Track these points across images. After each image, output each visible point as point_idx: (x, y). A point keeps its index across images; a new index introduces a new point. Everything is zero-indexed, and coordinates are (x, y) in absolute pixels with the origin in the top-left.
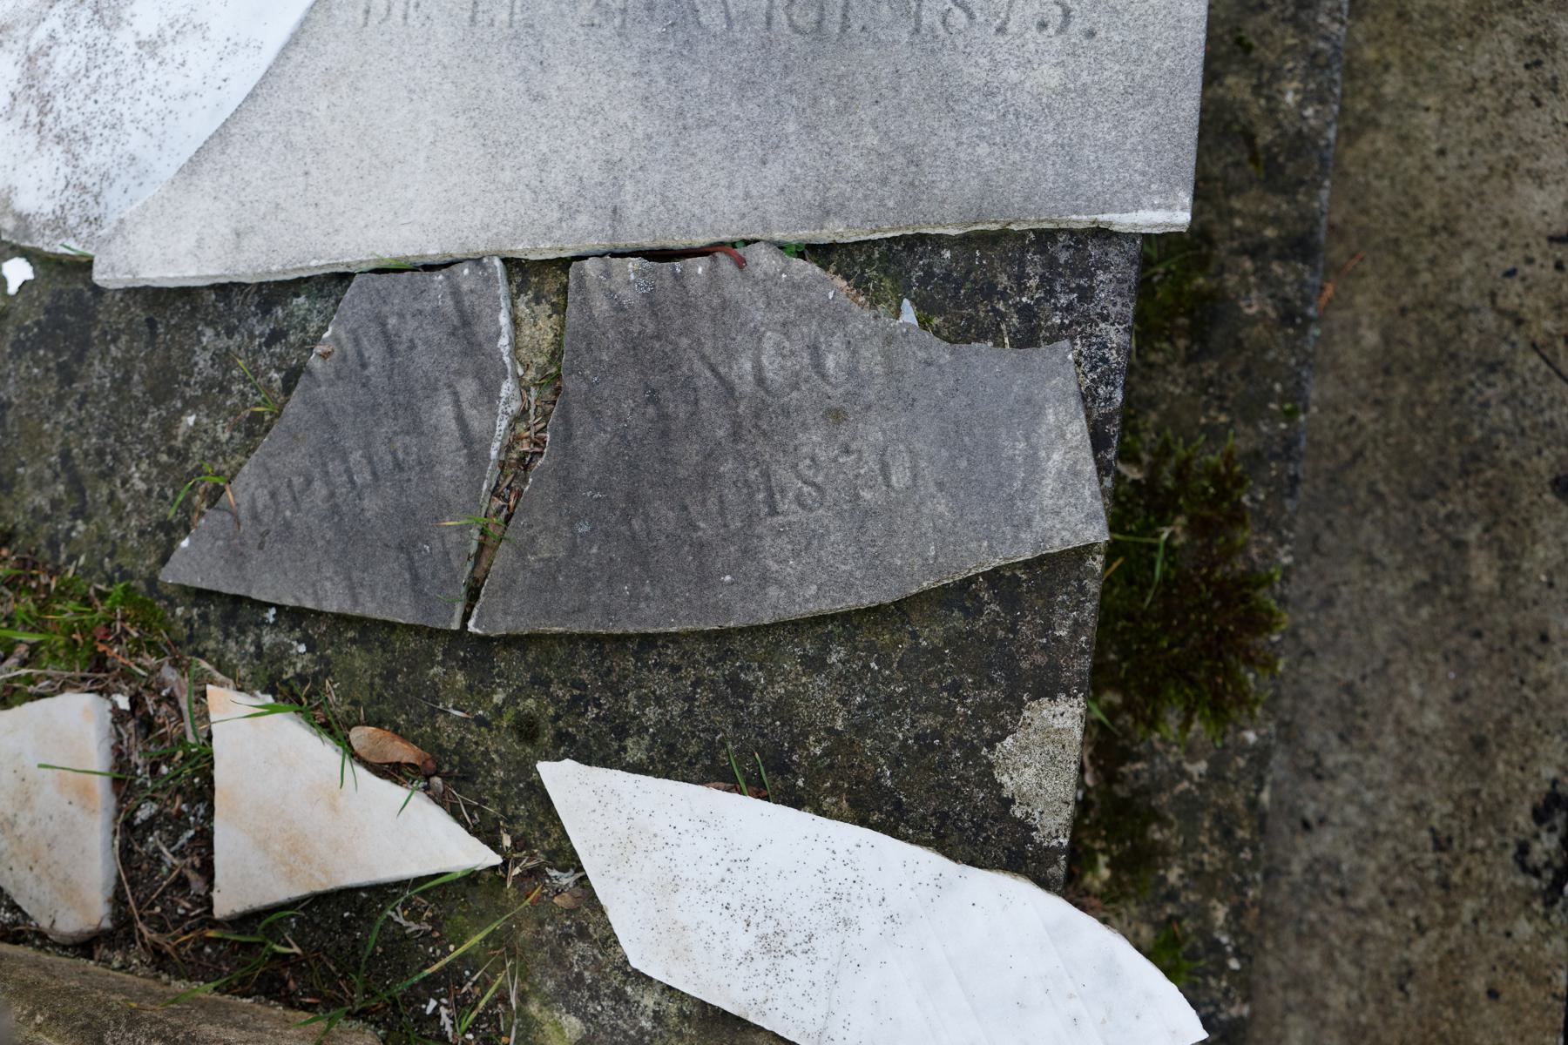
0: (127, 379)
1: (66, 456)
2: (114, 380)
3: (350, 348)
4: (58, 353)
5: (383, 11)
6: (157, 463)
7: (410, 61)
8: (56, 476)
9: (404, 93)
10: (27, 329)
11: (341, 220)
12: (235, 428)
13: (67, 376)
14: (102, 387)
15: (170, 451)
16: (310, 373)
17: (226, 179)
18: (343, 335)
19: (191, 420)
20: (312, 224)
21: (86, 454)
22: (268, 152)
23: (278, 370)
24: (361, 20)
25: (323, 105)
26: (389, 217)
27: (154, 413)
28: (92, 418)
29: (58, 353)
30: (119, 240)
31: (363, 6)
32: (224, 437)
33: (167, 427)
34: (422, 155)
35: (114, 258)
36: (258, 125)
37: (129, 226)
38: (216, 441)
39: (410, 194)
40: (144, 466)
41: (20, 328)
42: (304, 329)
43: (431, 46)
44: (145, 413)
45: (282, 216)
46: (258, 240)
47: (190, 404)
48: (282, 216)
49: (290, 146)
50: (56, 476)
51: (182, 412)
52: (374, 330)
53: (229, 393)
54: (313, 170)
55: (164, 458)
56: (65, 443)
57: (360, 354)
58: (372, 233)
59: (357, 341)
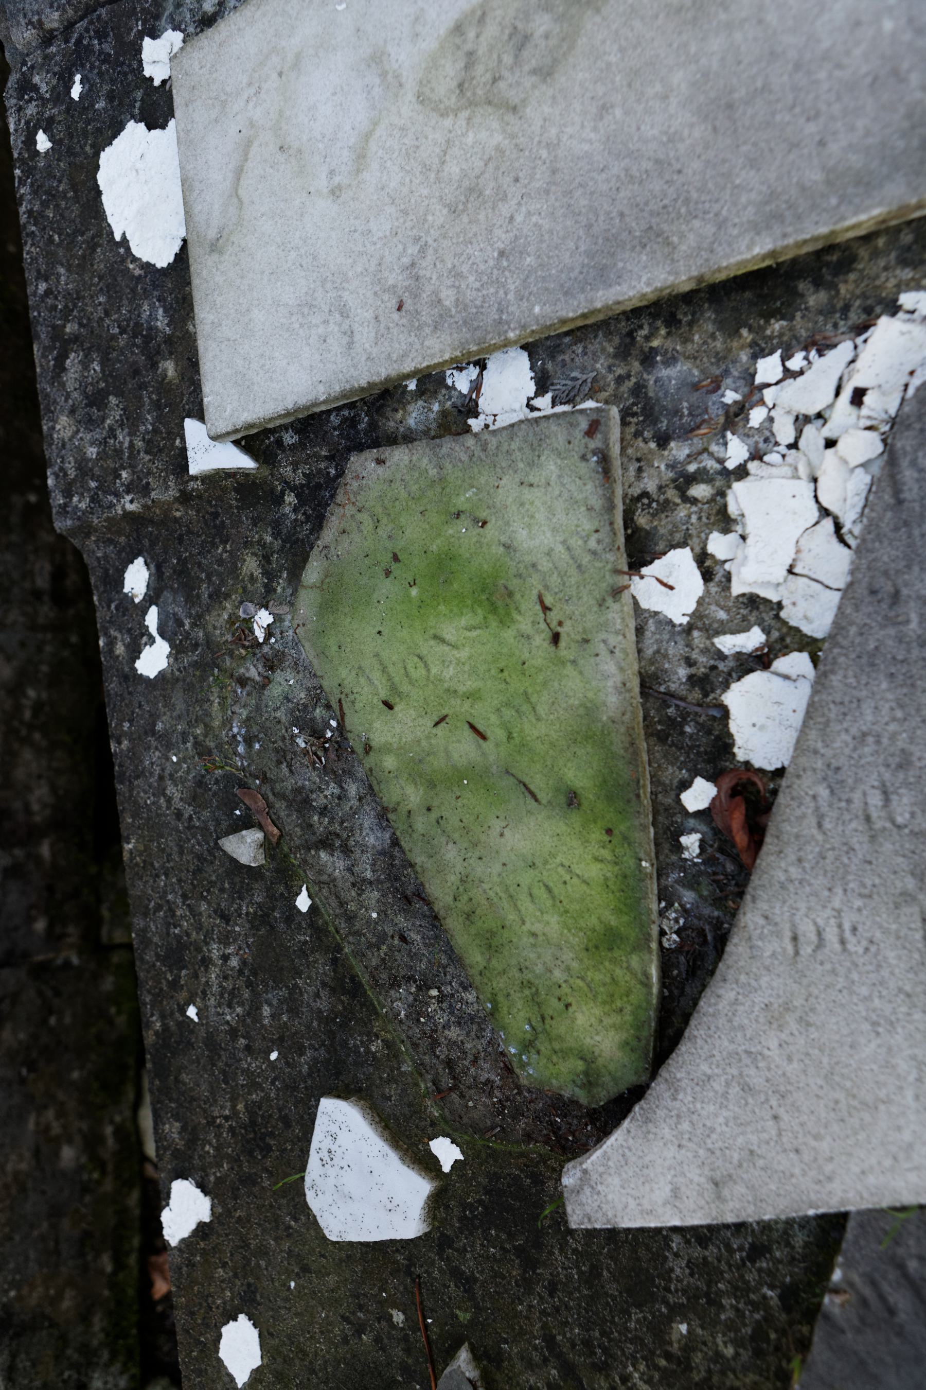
0: (595, 1271)
1: (549, 1340)
2: (580, 1273)
3: (867, 1292)
4: (511, 1236)
5: (813, 937)
6: (657, 1368)
7: (864, 991)
8: (546, 1360)
9: (866, 1027)
10: (471, 1206)
11: (828, 1168)
12: (738, 1343)
13: (530, 1263)
14: (569, 1277)
15: (668, 1356)
16: (827, 1317)
17: (685, 1126)
18: (856, 1279)
19: (684, 1328)
20: (797, 1171)
21: (573, 1345)
22: (725, 1095)
23: (772, 1287)
24: (790, 949)
25: (773, 1044)
26: (888, 1162)
27: (636, 1315)
28: (567, 1308)
29: (511, 1236)
30: (587, 1191)
31: (788, 934)
32: (729, 1351)
33: (659, 1328)
34: (909, 1094)
35: (588, 1209)
36: (704, 1067)
37: (594, 1176)
38: (718, 1355)
39: (907, 1136)
40: (642, 1367)
41: (464, 1206)
42: (788, 1244)
43: (885, 973)
44: (626, 1312)
45: (761, 1163)
46: (740, 1189)
47: (677, 1312)
48: (761, 1163)
49: (747, 1088)
50: (546, 1360)
51: (669, 1319)
52: (893, 1274)
53: (721, 1307)
54: (785, 1117)
55: (663, 1362)
56: (545, 1326)
57: (882, 1298)
58: (871, 1180)
59: (874, 1284)
